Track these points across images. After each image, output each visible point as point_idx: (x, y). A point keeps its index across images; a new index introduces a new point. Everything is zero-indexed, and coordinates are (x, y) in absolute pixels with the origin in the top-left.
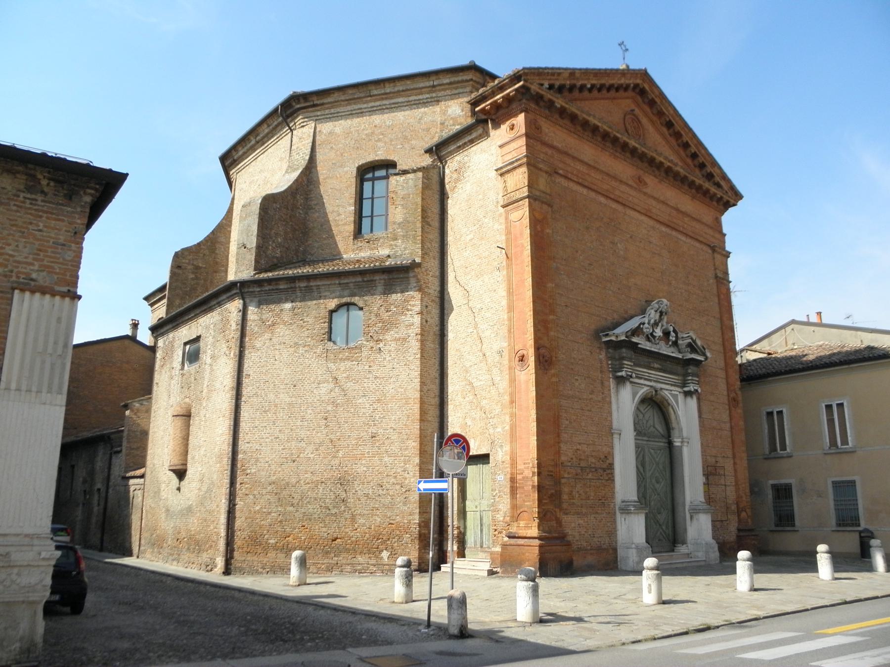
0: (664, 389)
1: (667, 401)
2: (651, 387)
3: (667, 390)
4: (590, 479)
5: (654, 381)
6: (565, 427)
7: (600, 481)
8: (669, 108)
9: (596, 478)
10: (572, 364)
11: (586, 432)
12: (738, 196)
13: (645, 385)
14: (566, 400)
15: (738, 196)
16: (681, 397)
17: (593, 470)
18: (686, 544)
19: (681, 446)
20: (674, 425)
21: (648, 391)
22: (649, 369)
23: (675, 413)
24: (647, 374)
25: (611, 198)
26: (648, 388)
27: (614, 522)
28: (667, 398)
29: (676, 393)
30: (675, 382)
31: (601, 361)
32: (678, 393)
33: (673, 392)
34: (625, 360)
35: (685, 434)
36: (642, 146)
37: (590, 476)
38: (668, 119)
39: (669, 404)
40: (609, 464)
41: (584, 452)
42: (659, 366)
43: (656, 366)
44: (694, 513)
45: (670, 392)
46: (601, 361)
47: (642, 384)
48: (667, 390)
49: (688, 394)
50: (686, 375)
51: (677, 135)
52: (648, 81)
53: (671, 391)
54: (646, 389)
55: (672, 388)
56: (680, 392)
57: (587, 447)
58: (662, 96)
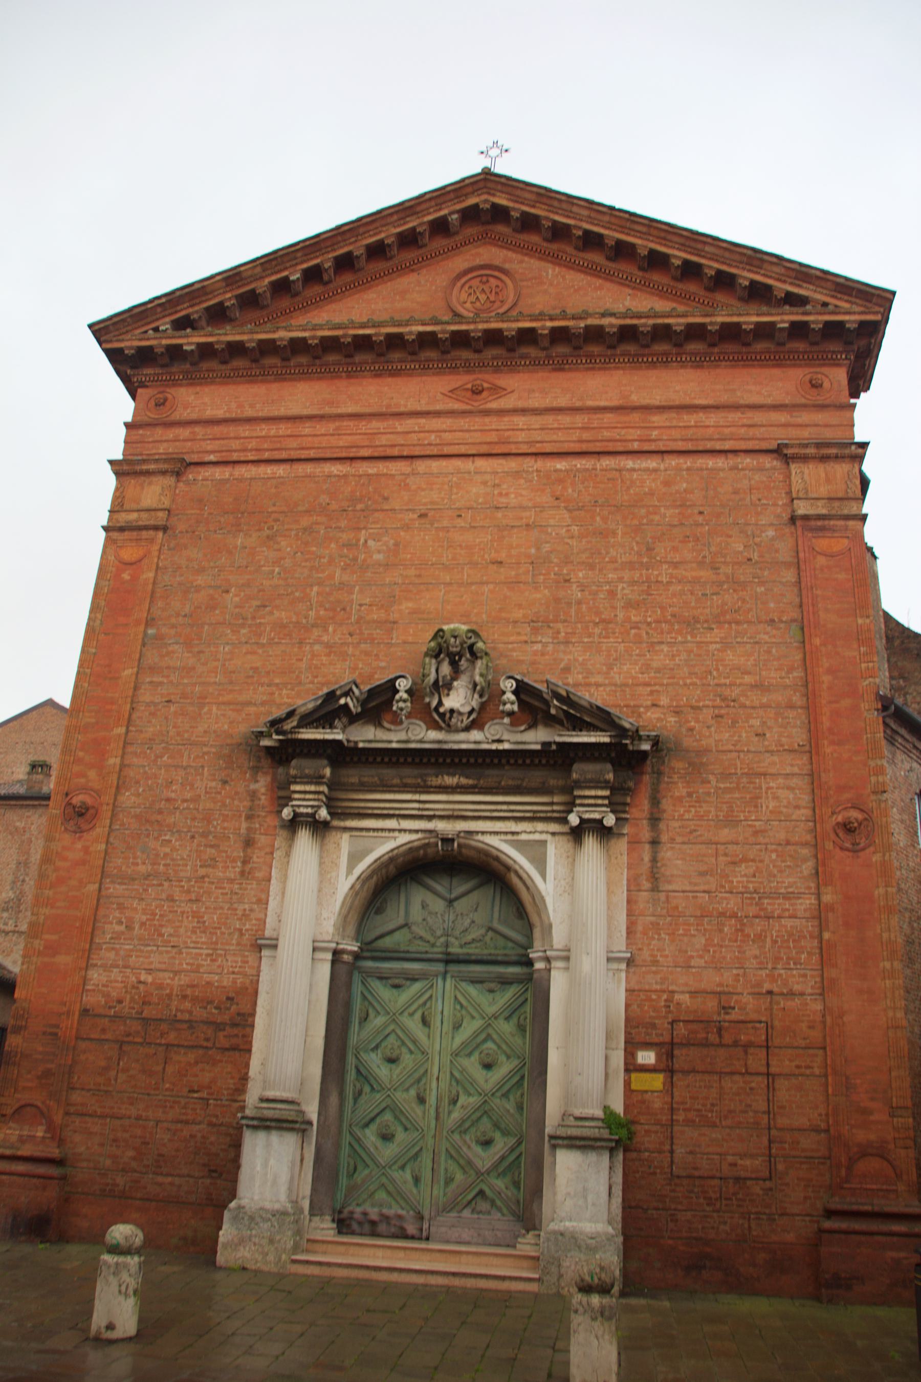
0: (483, 833)
1: (497, 859)
2: (430, 831)
3: (496, 833)
4: (168, 1045)
5: (441, 817)
6: (112, 938)
7: (201, 1052)
8: (575, 209)
9: (191, 1043)
10: (160, 812)
11: (173, 947)
12: (893, 293)
13: (400, 831)
14: (125, 884)
15: (893, 293)
16: (556, 850)
17: (185, 1026)
18: (535, 1228)
19: (549, 970)
20: (534, 918)
21: (416, 844)
22: (421, 793)
23: (528, 888)
24: (416, 805)
25: (364, 458)
26: (414, 837)
27: (237, 1145)
28: (495, 852)
29: (537, 837)
30: (535, 812)
31: (253, 795)
32: (548, 837)
33: (524, 837)
34: (296, 783)
35: (559, 938)
36: (475, 322)
37: (172, 1037)
38: (580, 233)
39: (508, 868)
40: (239, 1014)
41: (161, 987)
42: (471, 782)
43: (450, 780)
44: (248, 1126)
45: (509, 837)
46: (253, 795)
47: (390, 830)
48: (496, 833)
49: (577, 834)
50: (568, 790)
51: (622, 251)
52: (499, 187)
53: (513, 833)
54: (404, 838)
55: (512, 826)
56: (553, 834)
57: (173, 979)
58: (545, 195)
